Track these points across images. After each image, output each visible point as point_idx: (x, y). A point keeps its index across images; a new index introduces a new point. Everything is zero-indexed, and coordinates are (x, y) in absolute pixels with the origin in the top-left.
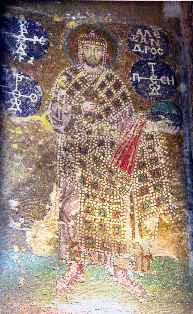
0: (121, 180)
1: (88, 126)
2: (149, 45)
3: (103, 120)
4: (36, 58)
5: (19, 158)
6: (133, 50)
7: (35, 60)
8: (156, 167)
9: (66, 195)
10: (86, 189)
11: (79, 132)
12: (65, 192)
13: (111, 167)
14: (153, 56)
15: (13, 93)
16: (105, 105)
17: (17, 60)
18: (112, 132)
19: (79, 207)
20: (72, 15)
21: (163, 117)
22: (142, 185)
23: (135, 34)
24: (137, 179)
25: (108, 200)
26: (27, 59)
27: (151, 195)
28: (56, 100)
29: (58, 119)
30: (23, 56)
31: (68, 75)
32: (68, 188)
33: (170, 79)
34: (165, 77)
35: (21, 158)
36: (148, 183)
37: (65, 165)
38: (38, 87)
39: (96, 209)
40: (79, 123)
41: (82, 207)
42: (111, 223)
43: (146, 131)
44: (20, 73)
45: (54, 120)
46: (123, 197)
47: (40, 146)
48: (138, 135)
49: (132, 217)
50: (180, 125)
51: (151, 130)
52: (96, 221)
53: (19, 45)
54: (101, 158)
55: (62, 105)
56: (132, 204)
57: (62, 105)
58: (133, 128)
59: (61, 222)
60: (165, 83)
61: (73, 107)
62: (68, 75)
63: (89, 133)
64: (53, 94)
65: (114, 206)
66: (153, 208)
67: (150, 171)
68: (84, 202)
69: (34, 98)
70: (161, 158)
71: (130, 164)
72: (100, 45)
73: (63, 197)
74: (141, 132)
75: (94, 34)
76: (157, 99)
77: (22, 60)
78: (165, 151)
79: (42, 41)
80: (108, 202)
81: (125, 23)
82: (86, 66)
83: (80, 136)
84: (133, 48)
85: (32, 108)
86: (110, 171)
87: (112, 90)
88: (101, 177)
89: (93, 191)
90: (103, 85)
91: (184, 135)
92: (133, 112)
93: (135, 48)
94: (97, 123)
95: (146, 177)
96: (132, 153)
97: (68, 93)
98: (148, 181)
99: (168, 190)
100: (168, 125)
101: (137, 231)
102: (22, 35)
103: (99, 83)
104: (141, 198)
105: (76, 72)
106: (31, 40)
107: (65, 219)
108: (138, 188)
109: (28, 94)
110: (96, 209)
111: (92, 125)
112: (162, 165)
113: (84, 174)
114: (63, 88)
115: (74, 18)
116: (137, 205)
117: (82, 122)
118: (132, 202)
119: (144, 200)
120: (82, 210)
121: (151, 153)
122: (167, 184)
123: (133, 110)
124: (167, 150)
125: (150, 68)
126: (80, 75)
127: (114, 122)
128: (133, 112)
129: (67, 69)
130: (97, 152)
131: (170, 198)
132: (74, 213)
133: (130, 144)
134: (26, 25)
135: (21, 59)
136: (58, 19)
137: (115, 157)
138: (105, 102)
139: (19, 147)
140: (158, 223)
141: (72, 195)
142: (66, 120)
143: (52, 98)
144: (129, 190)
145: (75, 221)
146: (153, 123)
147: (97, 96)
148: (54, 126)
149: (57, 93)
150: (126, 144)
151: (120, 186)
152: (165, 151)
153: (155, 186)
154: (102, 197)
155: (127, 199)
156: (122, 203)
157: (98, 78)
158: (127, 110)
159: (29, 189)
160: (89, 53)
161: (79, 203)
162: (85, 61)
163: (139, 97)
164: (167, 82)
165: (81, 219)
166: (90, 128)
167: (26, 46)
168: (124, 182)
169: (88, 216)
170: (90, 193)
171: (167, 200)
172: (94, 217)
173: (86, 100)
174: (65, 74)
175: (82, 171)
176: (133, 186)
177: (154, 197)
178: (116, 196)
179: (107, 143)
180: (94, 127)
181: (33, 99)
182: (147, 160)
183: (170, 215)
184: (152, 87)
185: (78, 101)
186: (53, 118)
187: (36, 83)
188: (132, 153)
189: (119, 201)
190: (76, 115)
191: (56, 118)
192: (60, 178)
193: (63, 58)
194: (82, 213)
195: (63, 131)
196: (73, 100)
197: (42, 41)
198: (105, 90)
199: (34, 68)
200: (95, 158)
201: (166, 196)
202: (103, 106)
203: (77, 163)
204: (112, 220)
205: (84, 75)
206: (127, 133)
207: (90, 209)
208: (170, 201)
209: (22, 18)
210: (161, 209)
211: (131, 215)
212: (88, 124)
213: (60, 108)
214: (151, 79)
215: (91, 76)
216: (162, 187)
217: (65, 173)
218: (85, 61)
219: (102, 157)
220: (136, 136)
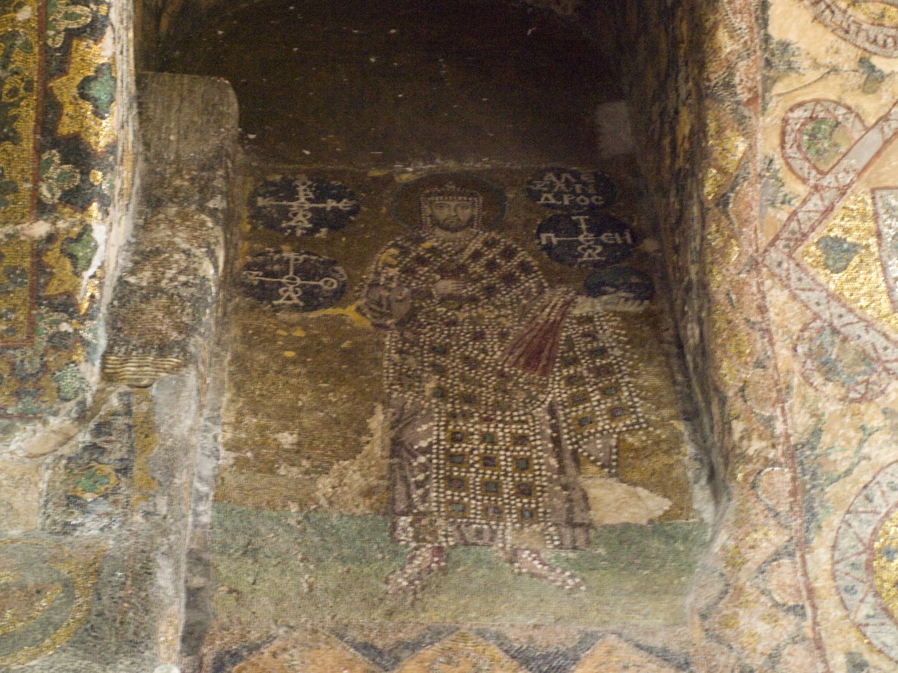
0: (526, 387)
1: (449, 314)
2: (573, 192)
3: (480, 304)
4: (332, 228)
5: (298, 370)
6: (539, 203)
7: (329, 232)
8: (604, 362)
9: (405, 417)
10: (449, 405)
11: (429, 324)
12: (402, 414)
13: (502, 370)
14: (580, 207)
15: (284, 280)
16: (484, 281)
17: (293, 233)
18: (503, 320)
19: (435, 433)
20: (409, 166)
21: (612, 290)
22: (575, 390)
23: (541, 179)
24: (562, 382)
25: (499, 418)
26: (311, 232)
27: (595, 403)
28: (378, 285)
29: (384, 310)
30: (305, 229)
31: (401, 247)
32: (408, 406)
33: (622, 235)
34: (610, 234)
35: (304, 371)
36: (587, 386)
37: (401, 374)
38: (339, 268)
39: (472, 434)
40: (430, 311)
41: (442, 433)
42: (508, 454)
43: (577, 312)
44: (298, 251)
45: (374, 311)
46: (534, 412)
47: (344, 351)
48: (559, 318)
49: (557, 441)
50: (650, 298)
51: (588, 309)
52: (476, 452)
53: (295, 215)
54: (480, 358)
55: (390, 290)
56: (554, 421)
57: (390, 290)
58: (548, 310)
59: (396, 460)
60: (611, 242)
61: (414, 291)
62: (401, 247)
63: (454, 323)
64: (372, 276)
65: (514, 426)
66: (601, 424)
67: (588, 369)
68: (446, 426)
69: (329, 284)
70: (612, 348)
71: (544, 362)
72: (467, 201)
73: (398, 421)
74: (564, 315)
75: (453, 187)
76: (596, 264)
77: (303, 235)
78: (621, 338)
79: (344, 205)
80: (500, 421)
81: (520, 167)
82: (439, 232)
83: (431, 330)
84: (539, 200)
85: (325, 298)
86: (502, 374)
87: (498, 261)
88: (481, 386)
89: (466, 408)
90: (476, 255)
91: (662, 311)
92: (545, 287)
93: (543, 199)
94: (468, 308)
95: (582, 377)
96: (548, 346)
97: (403, 271)
98: (588, 383)
99: (634, 394)
100: (623, 300)
101: (568, 462)
102: (303, 200)
103: (468, 252)
104: (574, 409)
105: (419, 241)
106: (321, 206)
107: (405, 455)
108: (565, 396)
109: (317, 278)
110: (472, 434)
111: (457, 313)
112: (616, 358)
113: (443, 383)
114: (391, 266)
115: (410, 169)
116: (565, 421)
117: (434, 310)
118: (552, 418)
119: (580, 413)
120: (442, 437)
121: (590, 342)
122: (631, 385)
123: (546, 284)
124: (625, 336)
125: (576, 224)
126: (427, 245)
127: (504, 305)
128: (545, 287)
129: (398, 239)
130: (470, 349)
131: (638, 405)
132: (424, 444)
133: (541, 334)
134: (310, 187)
135: (299, 232)
136: (376, 173)
137: (511, 354)
138: (483, 278)
139: (299, 355)
140: (616, 447)
141: (418, 417)
142: (402, 309)
143: (368, 282)
144: (545, 400)
145: (428, 456)
146: (590, 299)
147: (466, 272)
148: (374, 321)
149: (378, 274)
150: (534, 333)
151: (524, 396)
152: (621, 338)
153: (604, 392)
154: (485, 415)
155: (540, 412)
156: (530, 420)
157: (466, 246)
158: (533, 285)
159: (322, 414)
160: (443, 214)
161: (436, 428)
162: (437, 223)
163: (557, 266)
164: (615, 240)
165: (442, 452)
166: (453, 317)
167: (310, 215)
168: (533, 389)
169: (457, 445)
170: (458, 411)
171: (632, 410)
172: (471, 446)
173: (442, 278)
174: (395, 245)
175: (439, 379)
176: (554, 394)
177: (603, 406)
178: (517, 410)
179: (492, 334)
180: (462, 315)
181: (328, 284)
182: (583, 353)
183: (641, 432)
184: (584, 250)
185: (424, 282)
186: (371, 309)
187: (334, 263)
188: (548, 346)
189: (523, 418)
190: (423, 300)
191: (378, 309)
192: (390, 393)
193: (389, 224)
194: (443, 443)
195: (393, 327)
196: (416, 281)
197: (344, 205)
198: (483, 261)
199: (328, 242)
200: (466, 359)
201: (630, 403)
202: (478, 284)
203: (427, 369)
204: (511, 448)
205: (436, 244)
206: (534, 318)
207: (459, 436)
208: (639, 410)
209: (303, 177)
210: (621, 424)
211: (552, 438)
212: (447, 312)
213: (385, 293)
214: (581, 238)
215: (451, 244)
216: (617, 388)
217: (402, 385)
218: (437, 223)
219: (482, 355)
220: (555, 321)
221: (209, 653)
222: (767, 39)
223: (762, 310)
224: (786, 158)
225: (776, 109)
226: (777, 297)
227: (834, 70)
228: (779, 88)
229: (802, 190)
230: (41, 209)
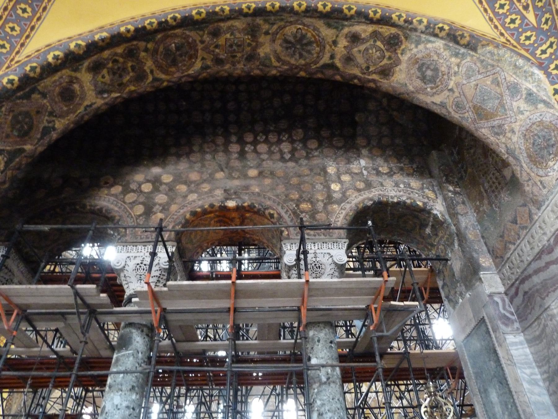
221: (491, 252)
222: (439, 105)
223: (484, 135)
224: (460, 114)
225: (451, 110)
226: (483, 130)
227: (448, 96)
228: (448, 107)
229: (467, 114)
230: (429, 217)
